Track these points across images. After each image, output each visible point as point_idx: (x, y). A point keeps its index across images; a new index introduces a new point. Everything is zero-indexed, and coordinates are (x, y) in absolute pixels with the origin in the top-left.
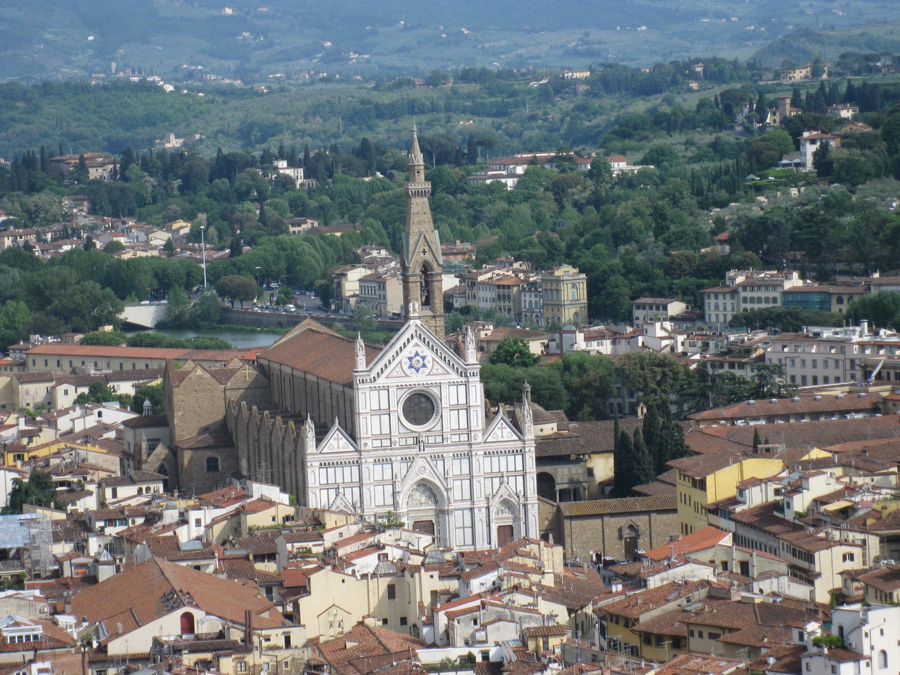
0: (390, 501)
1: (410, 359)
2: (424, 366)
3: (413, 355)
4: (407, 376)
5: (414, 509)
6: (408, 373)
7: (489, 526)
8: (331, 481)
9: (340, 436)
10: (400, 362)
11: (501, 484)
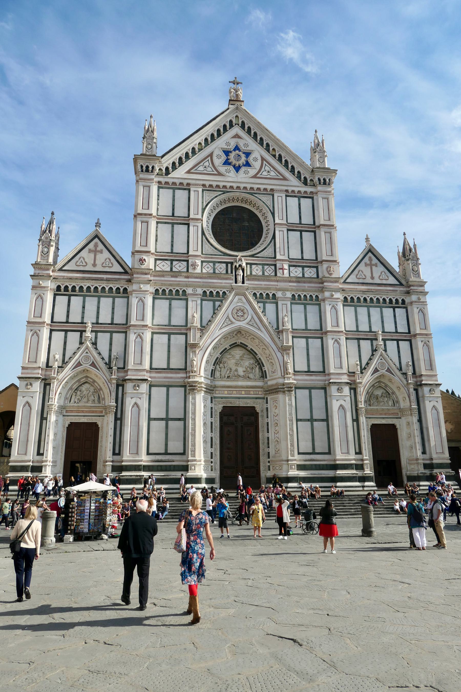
0: (176, 362)
2: (248, 164)
4: (220, 174)
6: (222, 169)
7: (356, 420)
8: (75, 317)
9: (101, 246)
10: (211, 155)
11: (374, 351)
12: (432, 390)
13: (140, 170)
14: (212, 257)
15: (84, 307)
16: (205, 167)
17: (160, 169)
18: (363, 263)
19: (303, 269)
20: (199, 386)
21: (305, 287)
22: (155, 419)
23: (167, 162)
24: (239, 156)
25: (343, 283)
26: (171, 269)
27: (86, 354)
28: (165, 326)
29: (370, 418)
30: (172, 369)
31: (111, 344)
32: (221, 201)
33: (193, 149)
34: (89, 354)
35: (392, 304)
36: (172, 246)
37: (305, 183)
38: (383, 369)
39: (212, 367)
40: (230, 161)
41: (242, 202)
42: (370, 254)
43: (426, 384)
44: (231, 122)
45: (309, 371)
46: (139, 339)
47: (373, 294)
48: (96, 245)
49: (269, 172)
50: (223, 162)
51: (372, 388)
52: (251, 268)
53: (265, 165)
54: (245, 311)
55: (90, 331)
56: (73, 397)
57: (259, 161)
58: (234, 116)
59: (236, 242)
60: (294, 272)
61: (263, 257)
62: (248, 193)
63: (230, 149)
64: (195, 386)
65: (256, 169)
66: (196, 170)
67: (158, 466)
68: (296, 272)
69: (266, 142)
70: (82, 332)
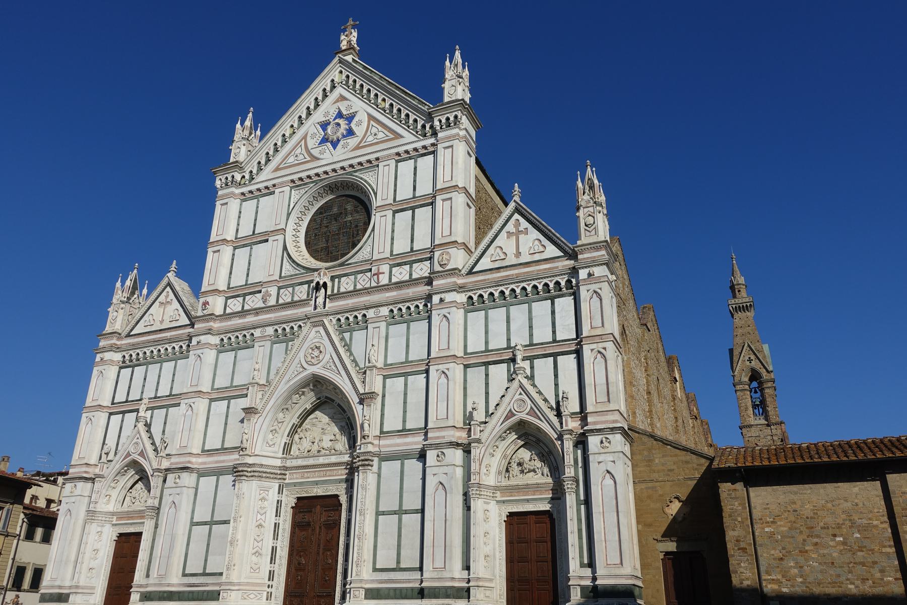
1: (324, 126)
3: (331, 117)
5: (300, 462)
6: (315, 152)
9: (172, 296)
10: (305, 138)
11: (511, 380)
12: (604, 439)
14: (291, 279)
15: (145, 379)
16: (296, 156)
17: (244, 177)
18: (503, 234)
19: (411, 267)
20: (249, 470)
21: (409, 293)
22: (198, 524)
24: (338, 125)
25: (467, 275)
26: (243, 307)
27: (138, 440)
28: (226, 388)
29: (504, 502)
30: (226, 449)
31: (165, 423)
32: (313, 197)
34: (139, 441)
35: (549, 291)
36: (248, 275)
37: (425, 135)
38: (523, 410)
39: (285, 439)
41: (343, 188)
42: (517, 216)
43: (592, 431)
45: (404, 430)
46: (190, 412)
47: (514, 283)
48: (167, 296)
50: (319, 141)
51: (513, 446)
52: (339, 282)
53: (372, 125)
54: (321, 349)
55: (145, 409)
56: (127, 499)
57: (365, 124)
59: (334, 248)
60: (397, 274)
61: (356, 263)
62: (346, 174)
63: (329, 120)
64: (242, 471)
65: (357, 136)
66: (285, 164)
67: (190, 592)
68: (401, 273)
70: (137, 411)
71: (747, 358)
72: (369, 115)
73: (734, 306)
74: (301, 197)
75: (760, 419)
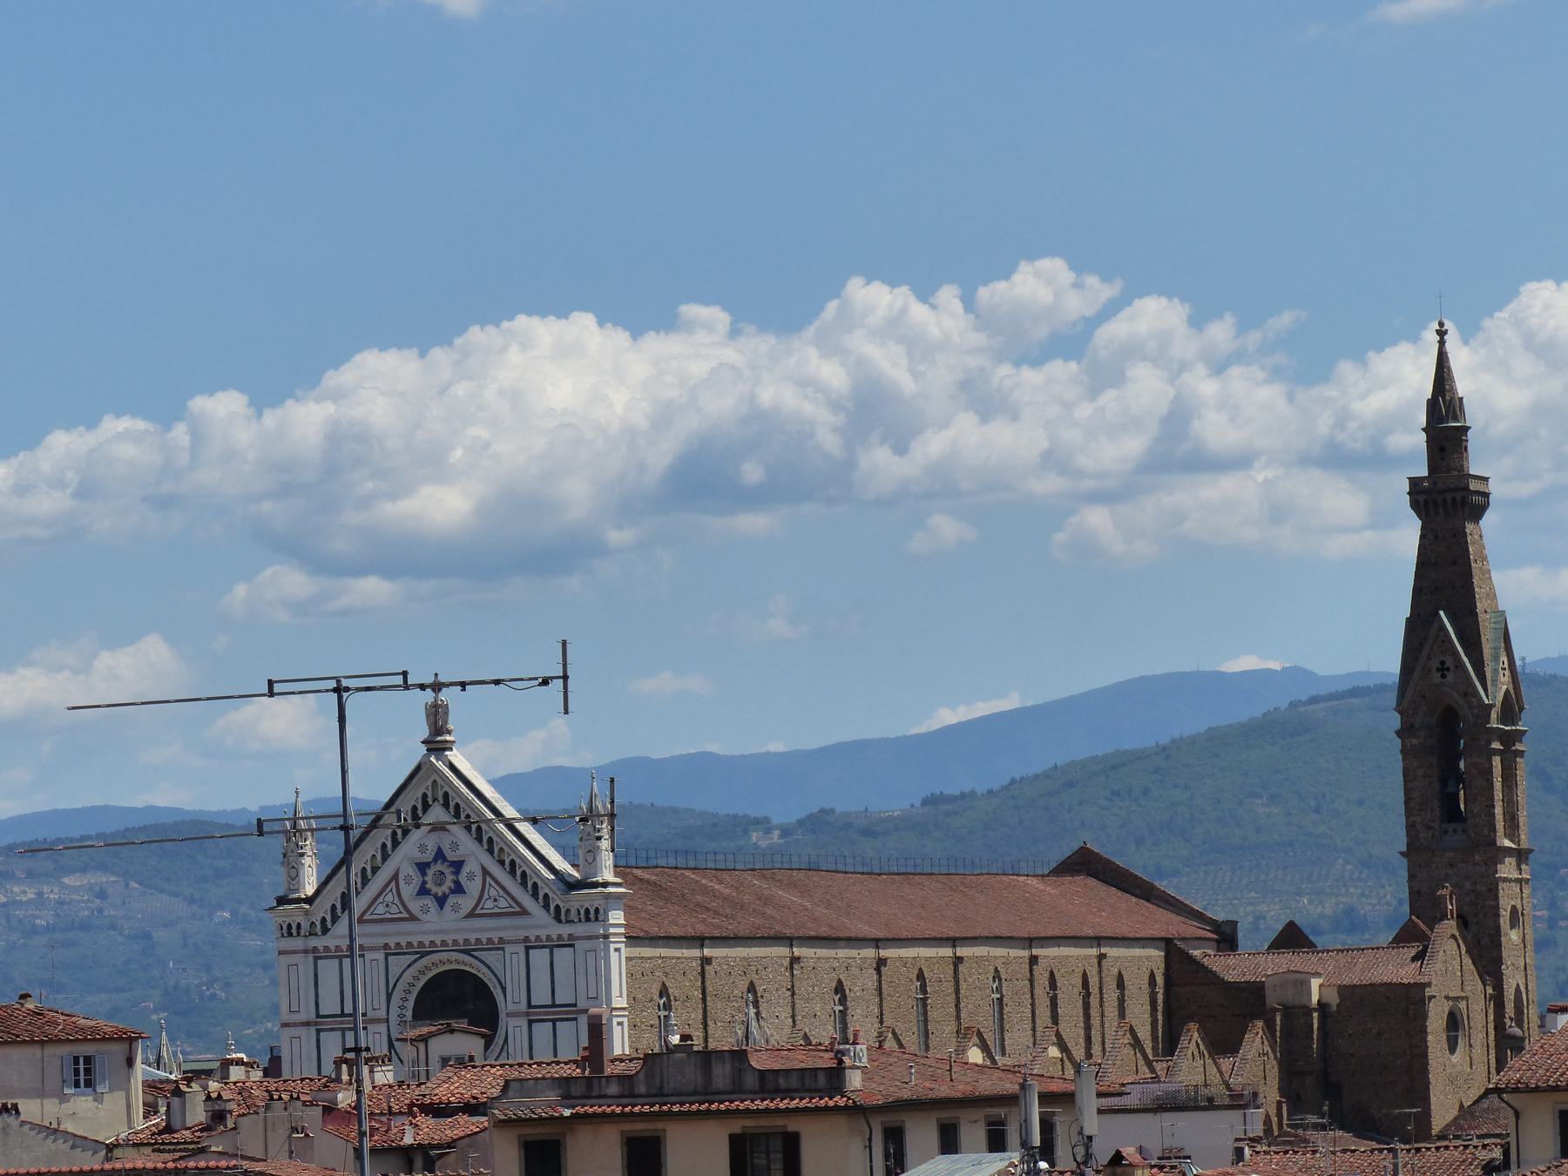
1: (422, 867)
2: (458, 889)
3: (428, 856)
4: (412, 918)
6: (415, 906)
10: (395, 877)
13: (279, 935)
23: (321, 910)
24: (442, 873)
33: (364, 869)
37: (560, 921)
40: (428, 886)
44: (425, 796)
49: (495, 900)
57: (478, 881)
58: (429, 783)
69: (487, 837)
71: (1435, 664)
72: (482, 866)
73: (1421, 498)
74: (403, 972)
75: (1455, 831)
